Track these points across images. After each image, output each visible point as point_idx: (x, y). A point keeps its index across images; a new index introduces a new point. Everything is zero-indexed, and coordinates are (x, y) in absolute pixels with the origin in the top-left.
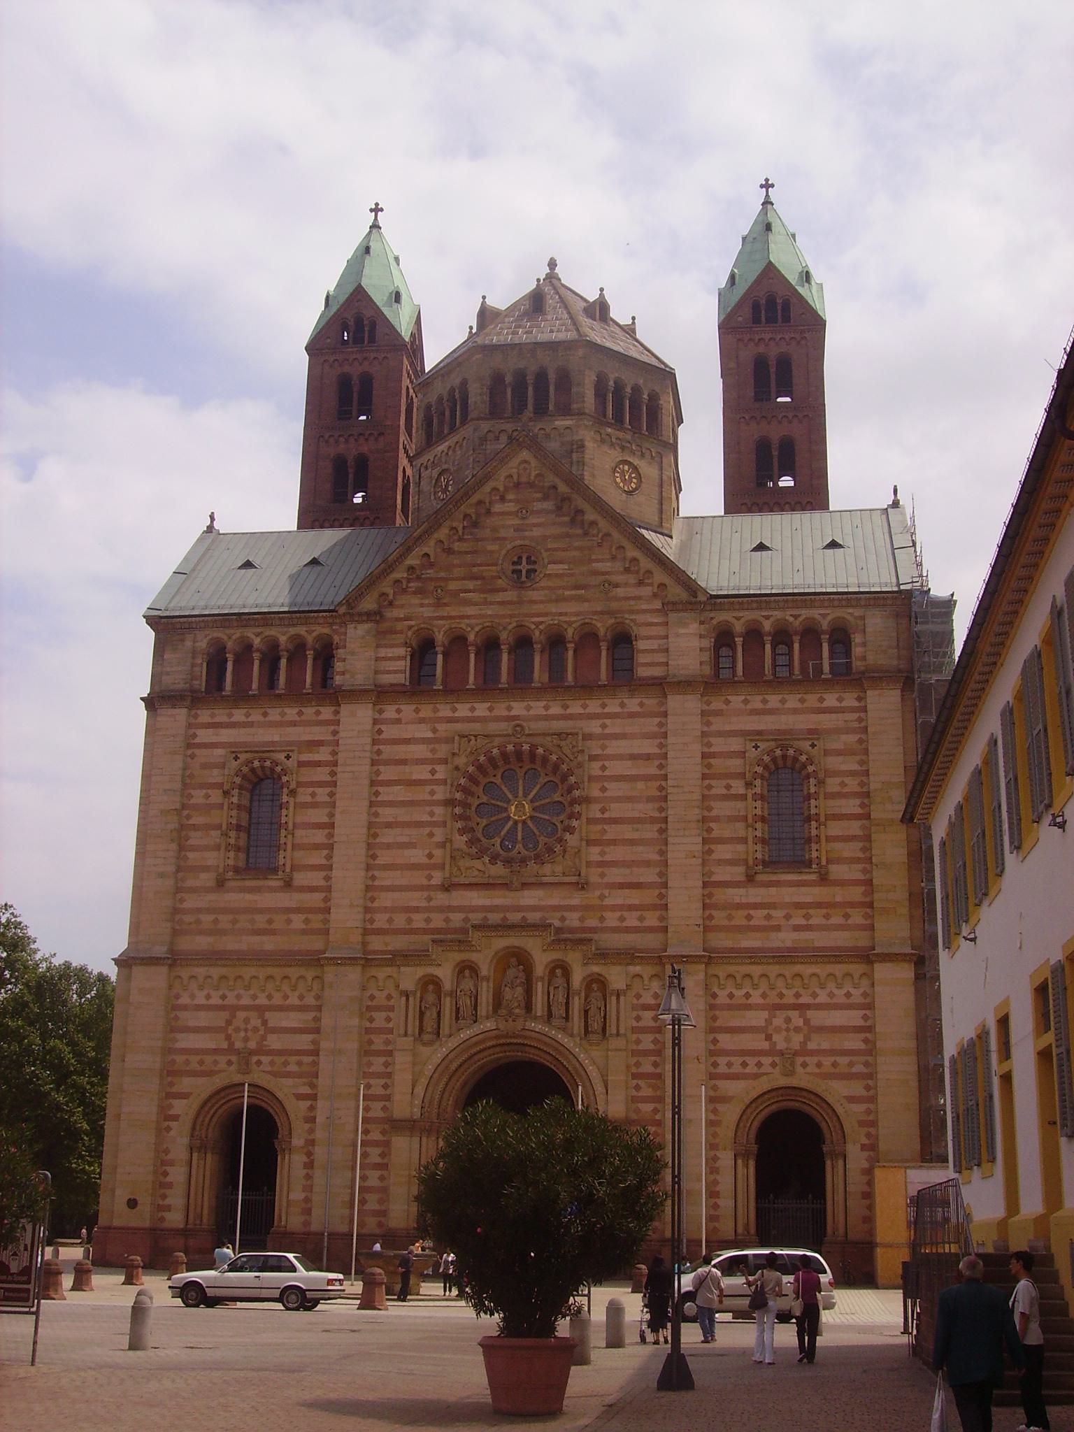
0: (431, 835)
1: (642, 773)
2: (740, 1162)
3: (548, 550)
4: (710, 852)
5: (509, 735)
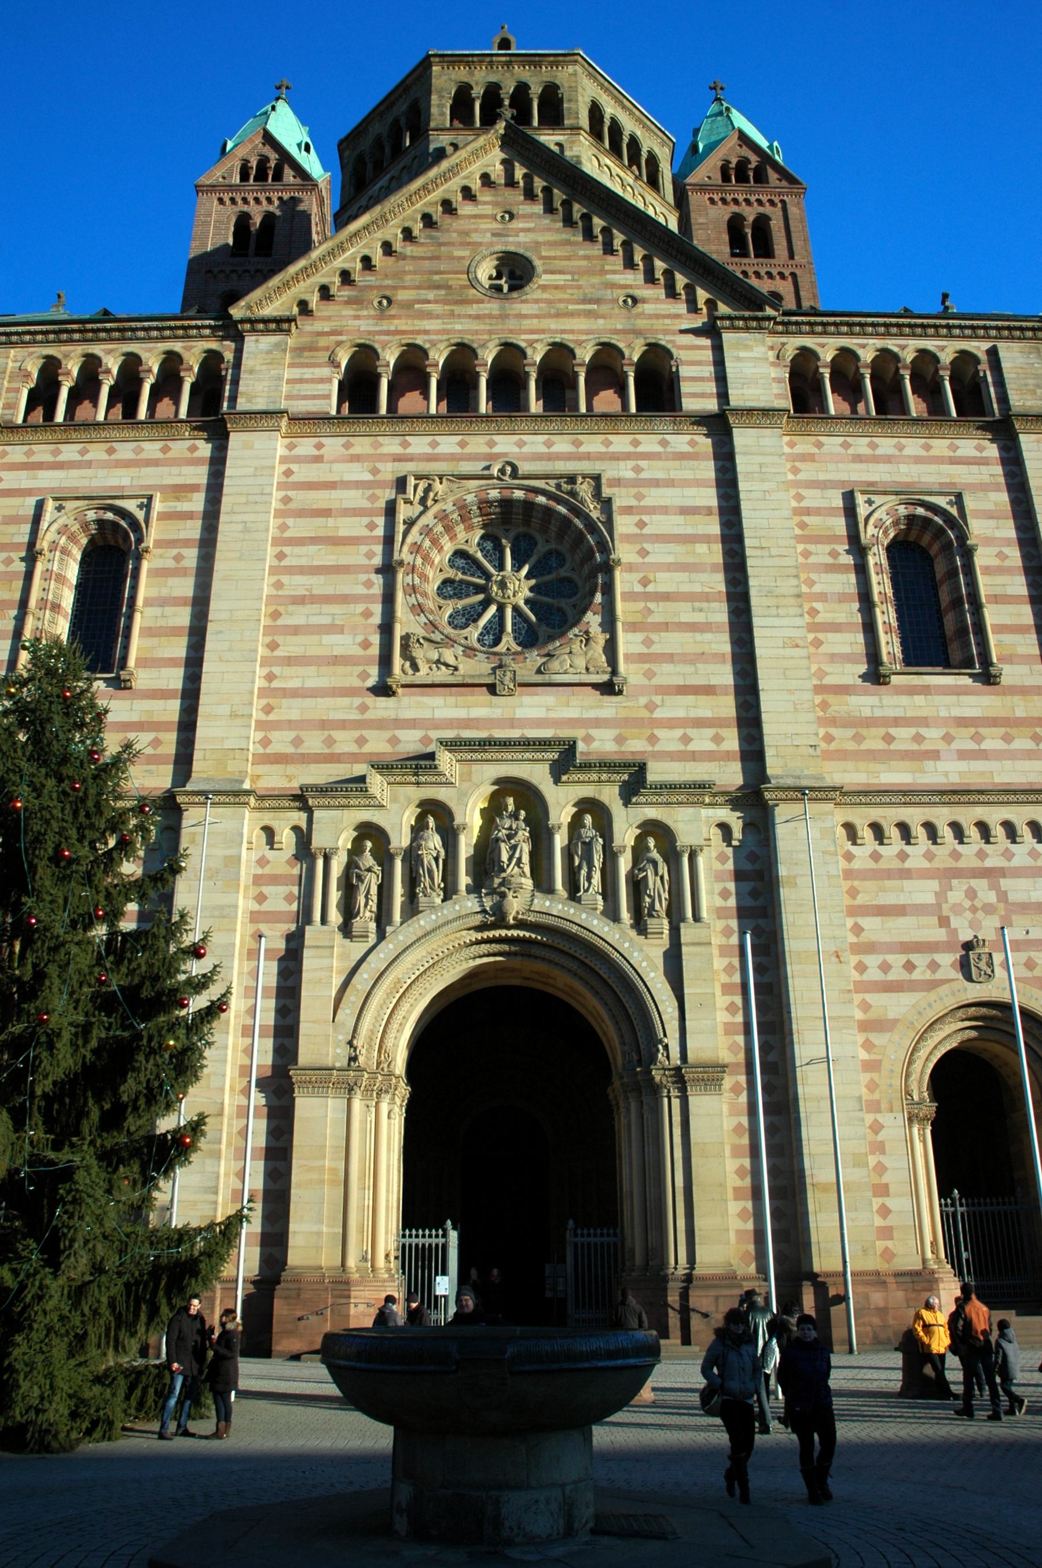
0: (367, 614)
1: (700, 532)
2: (915, 1130)
3: (542, 258)
4: (817, 643)
5: (490, 477)
